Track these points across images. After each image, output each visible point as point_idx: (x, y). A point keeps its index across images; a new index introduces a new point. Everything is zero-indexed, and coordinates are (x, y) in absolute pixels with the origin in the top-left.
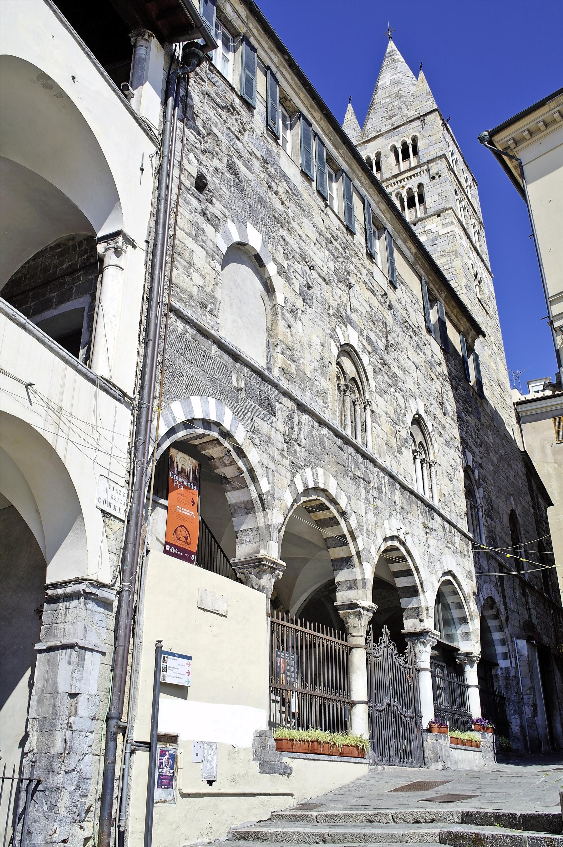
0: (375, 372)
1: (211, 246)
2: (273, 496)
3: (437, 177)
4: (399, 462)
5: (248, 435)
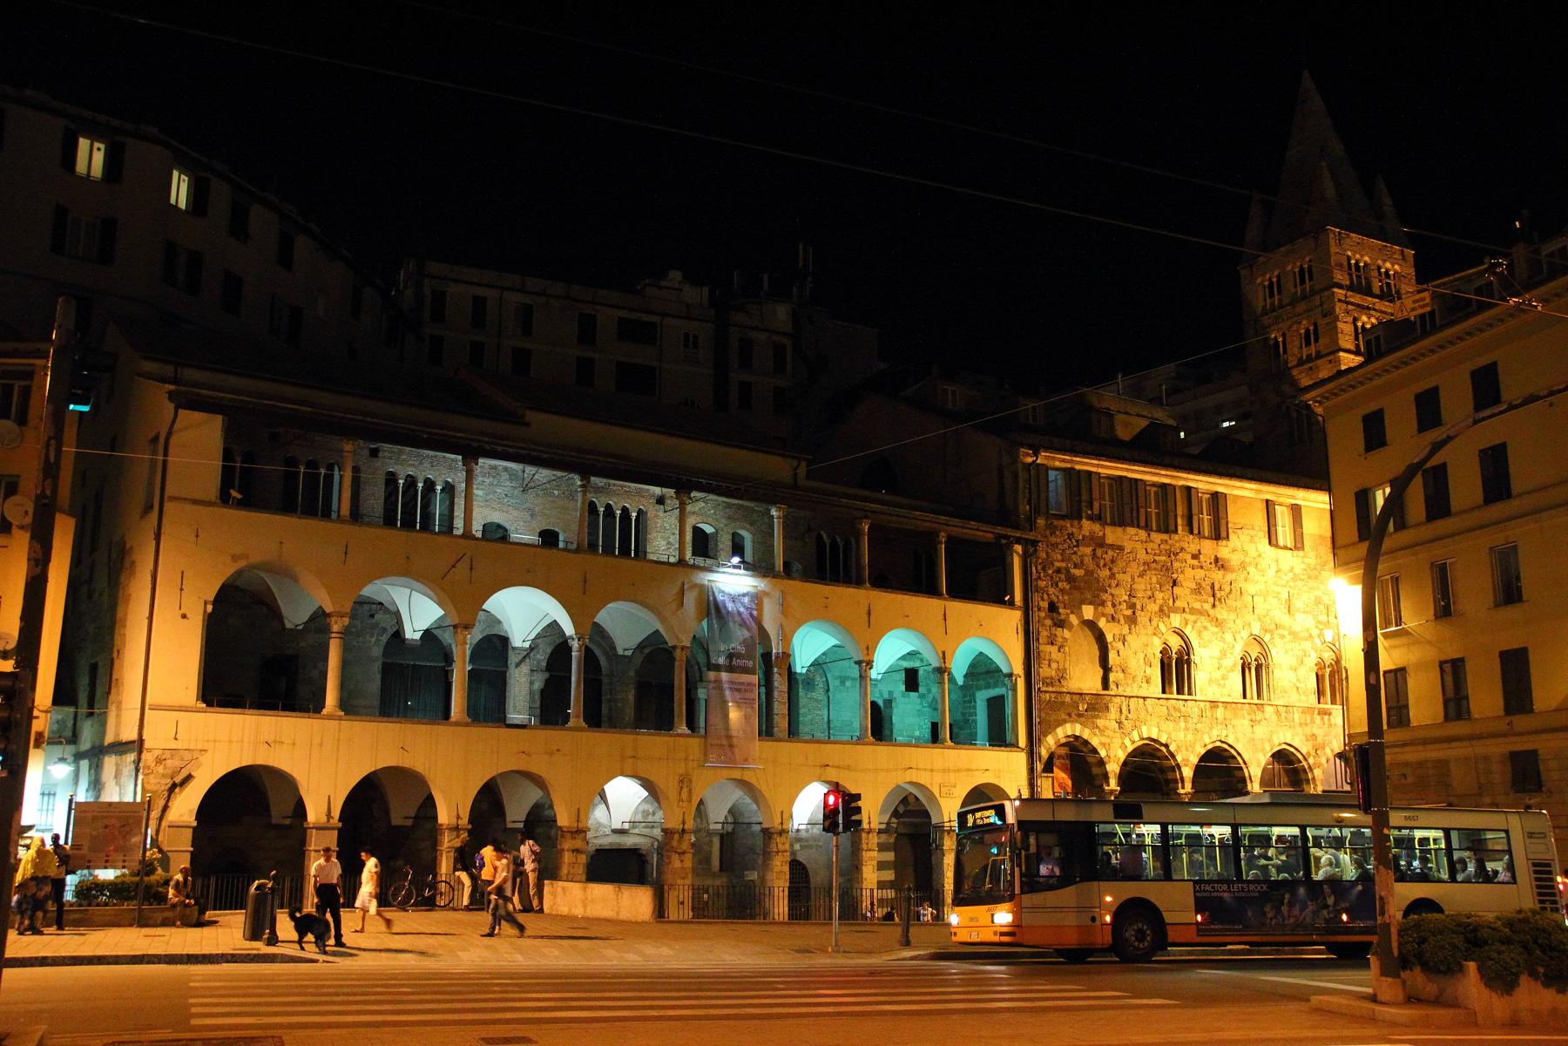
1: (1060, 640)
4: (1224, 686)
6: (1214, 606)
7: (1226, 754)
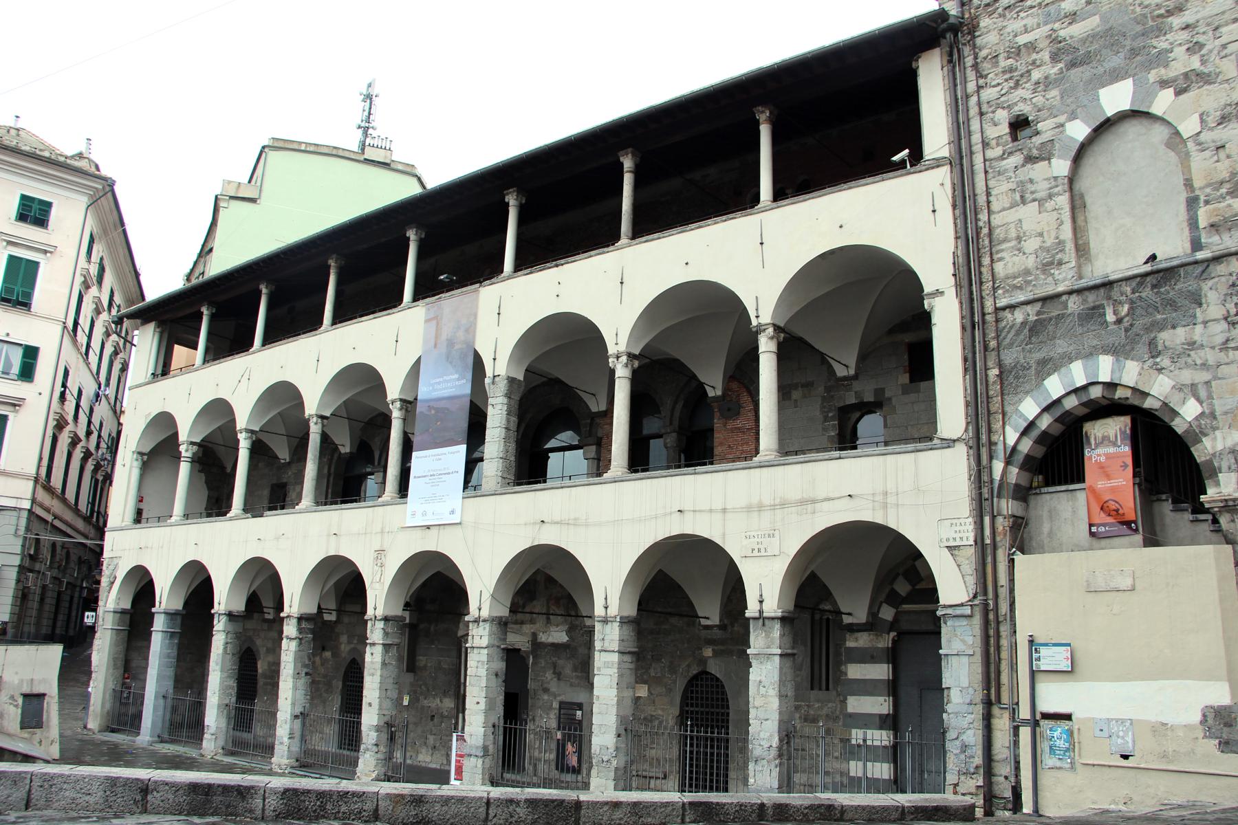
2: (1213, 415)
5: (1146, 367)
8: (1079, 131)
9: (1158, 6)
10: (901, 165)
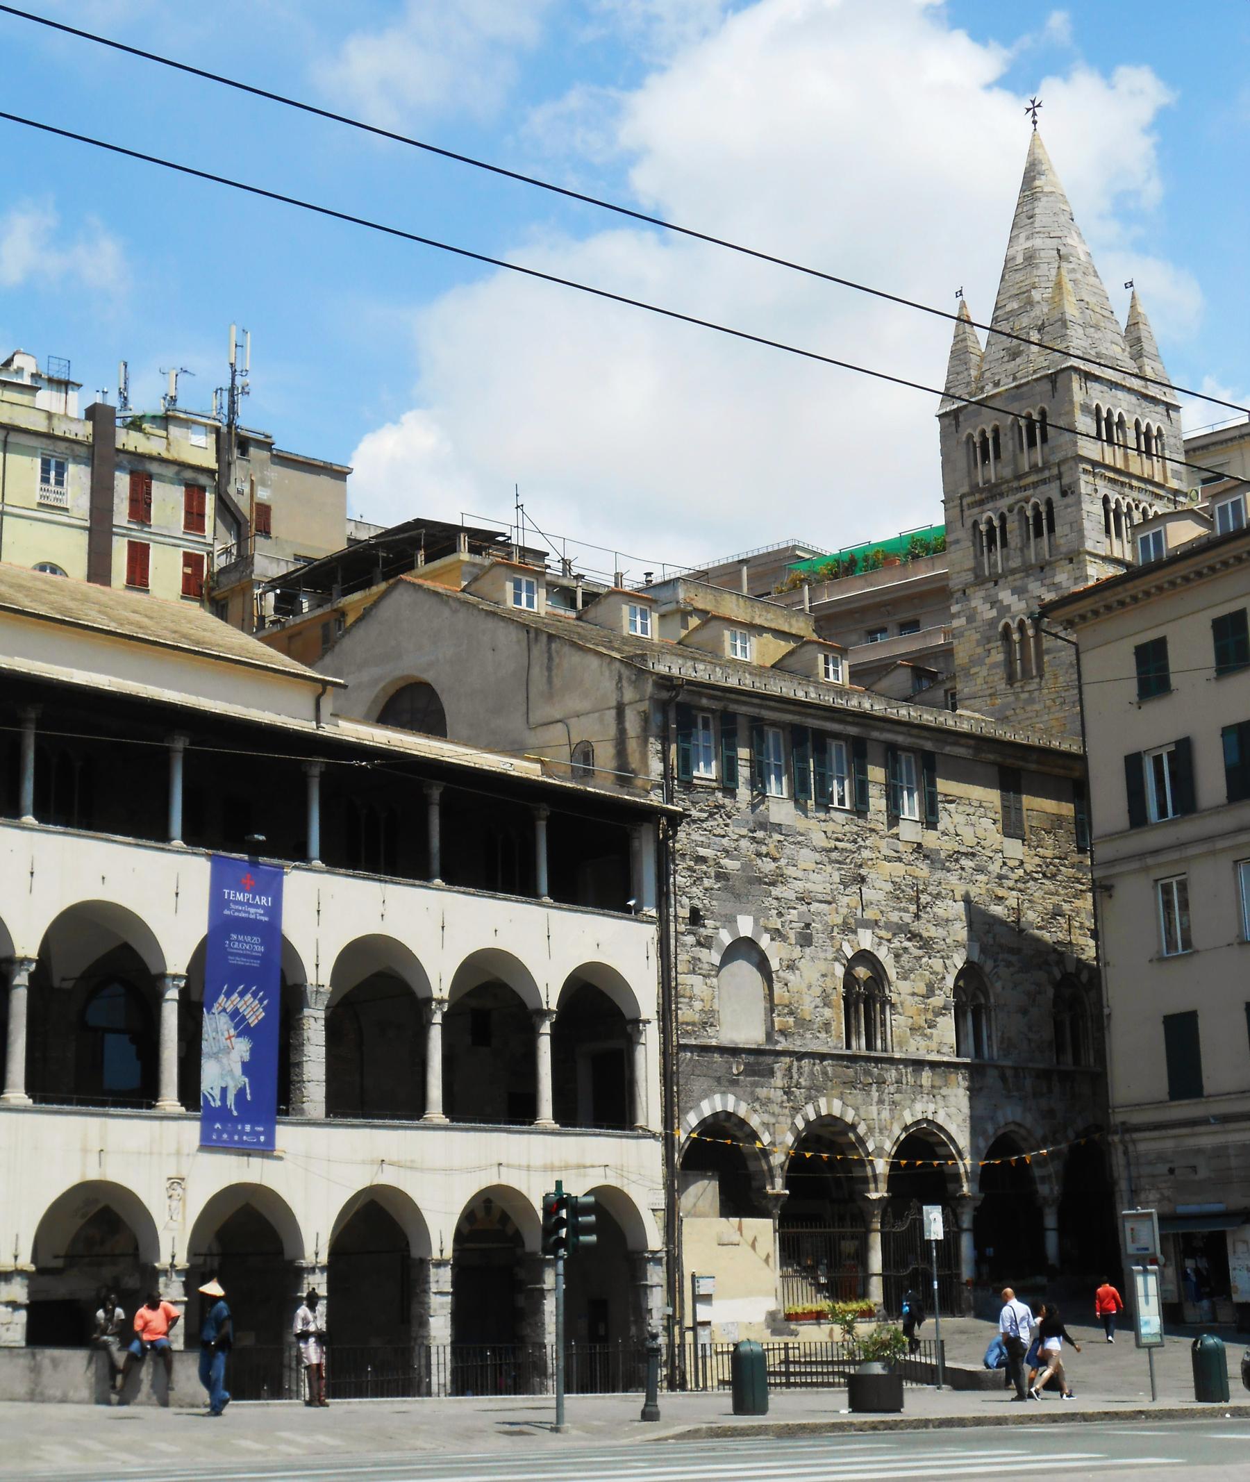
0: (897, 956)
1: (706, 966)
3: (1069, 492)
4: (930, 1037)
6: (917, 917)
7: (932, 1139)
8: (726, 938)
9: (766, 876)
10: (628, 910)
